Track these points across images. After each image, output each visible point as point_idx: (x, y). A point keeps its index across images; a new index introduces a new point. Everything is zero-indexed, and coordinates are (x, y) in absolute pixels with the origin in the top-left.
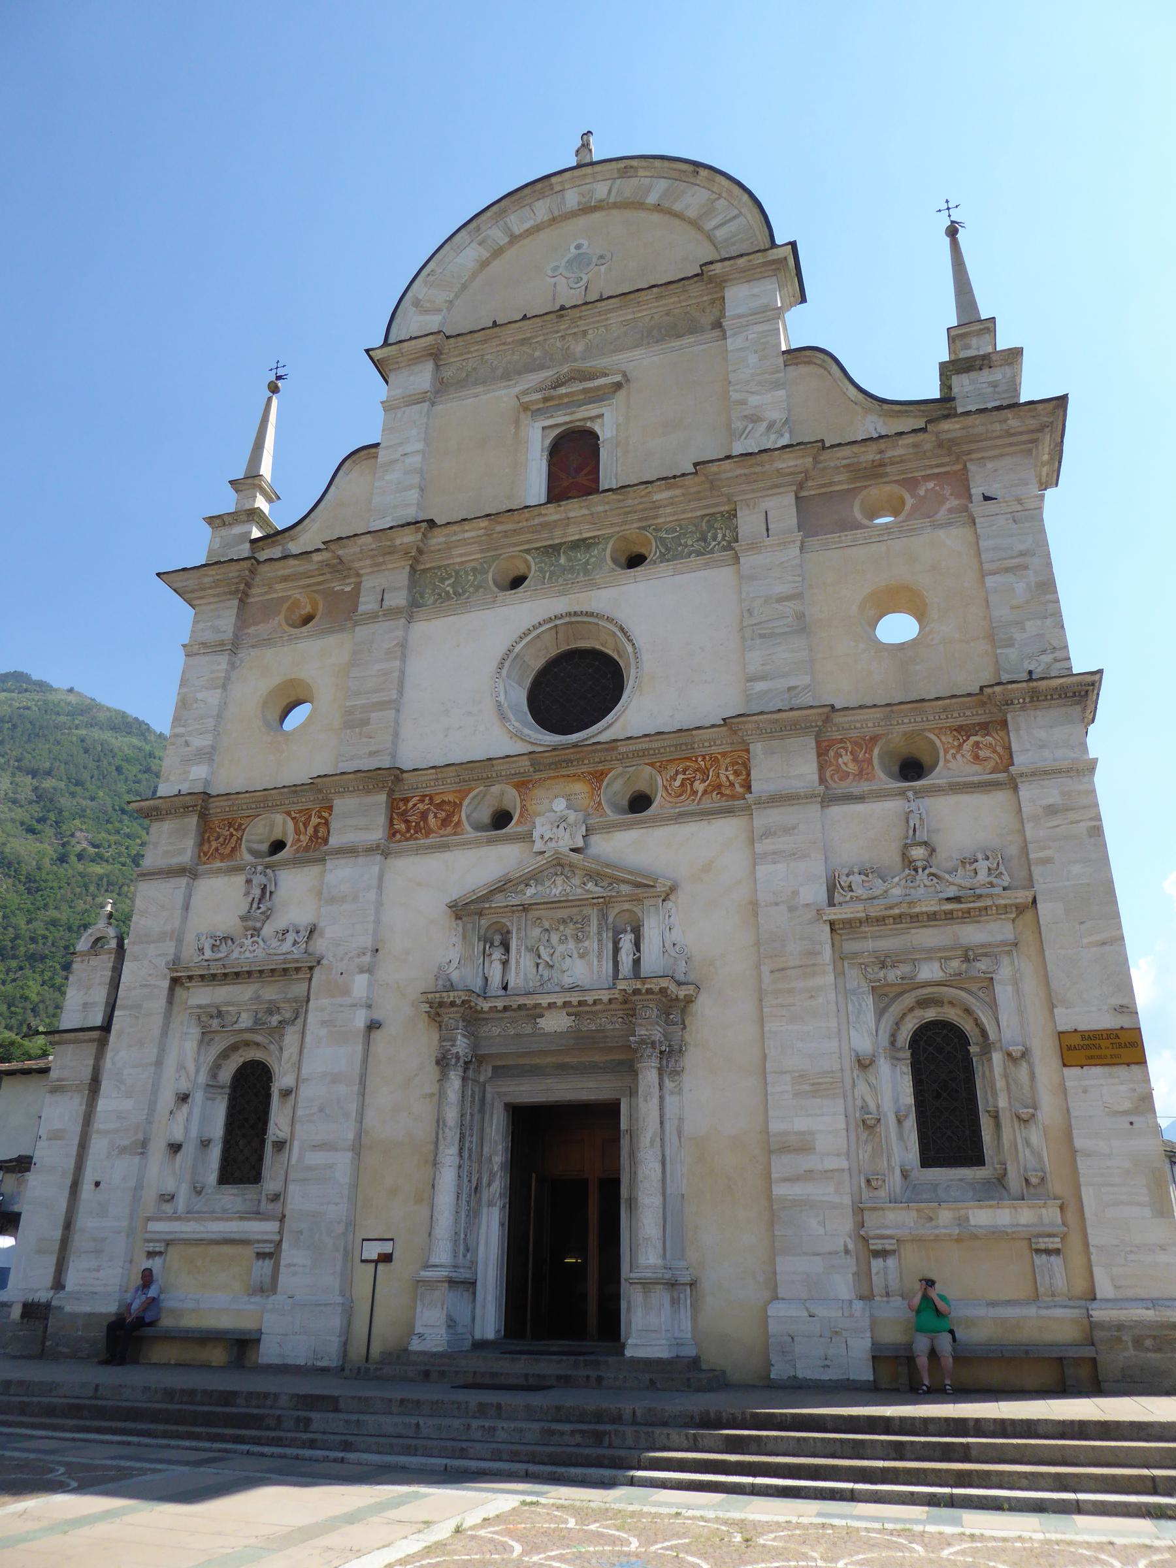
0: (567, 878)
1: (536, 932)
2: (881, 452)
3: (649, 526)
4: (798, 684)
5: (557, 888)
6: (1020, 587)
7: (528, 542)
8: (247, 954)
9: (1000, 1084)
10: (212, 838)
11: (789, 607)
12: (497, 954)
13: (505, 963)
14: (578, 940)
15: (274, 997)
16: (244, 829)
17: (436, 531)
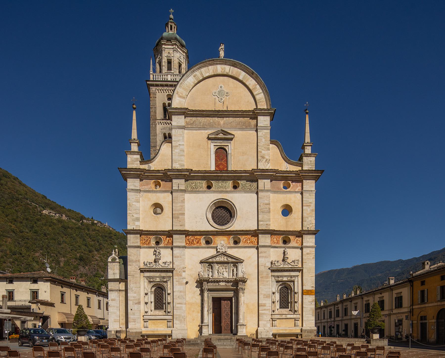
1: (218, 266)
5: (223, 259)
6: (309, 210)
11: (267, 206)
12: (210, 270)
14: (226, 269)
15: (164, 276)
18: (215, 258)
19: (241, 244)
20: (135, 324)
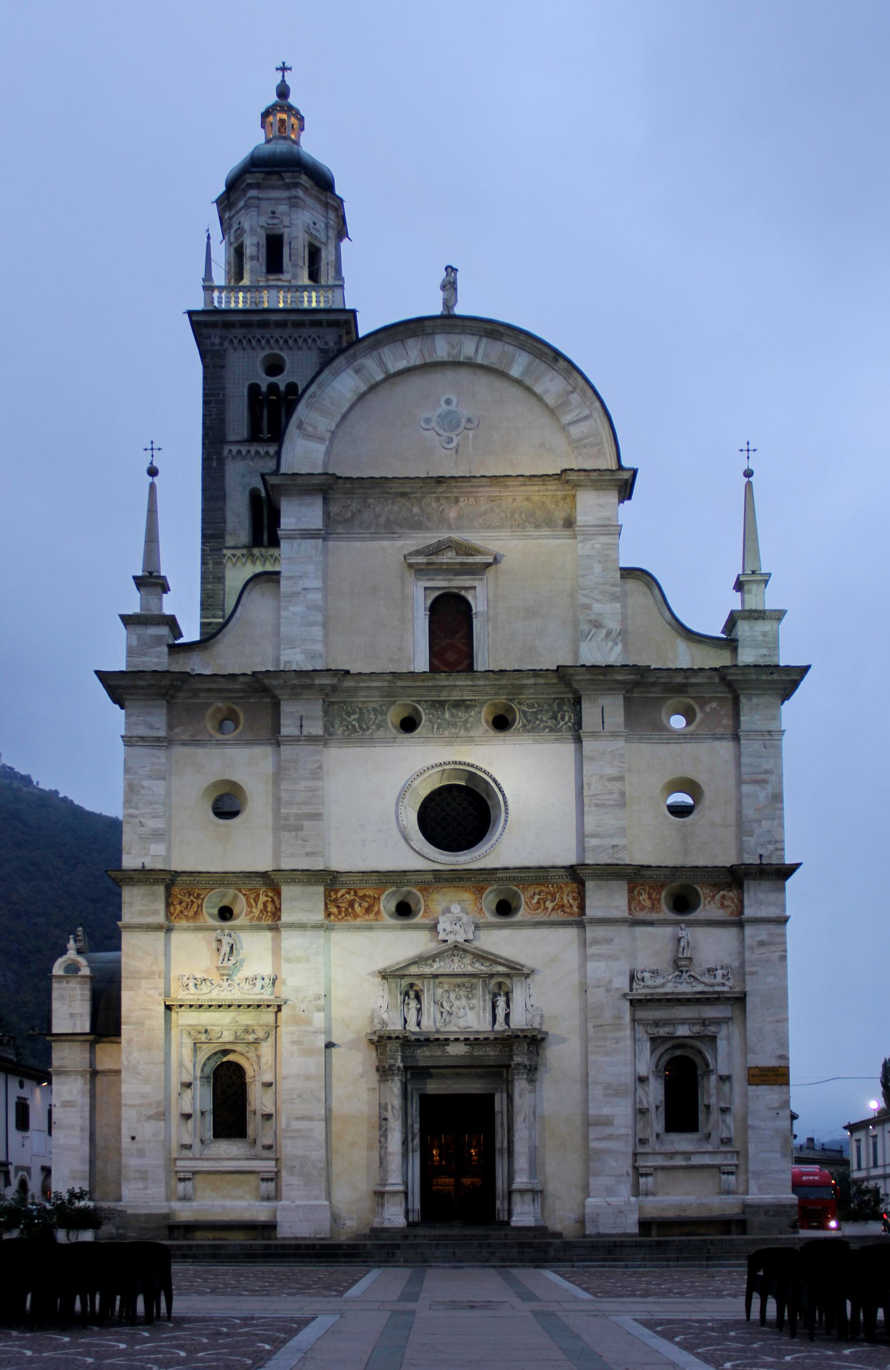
0: (461, 957)
2: (687, 678)
3: (515, 699)
5: (456, 966)
6: (762, 795)
7: (421, 696)
9: (713, 1092)
10: (175, 903)
11: (616, 786)
12: (413, 1004)
13: (419, 1010)
14: (468, 998)
16: (203, 899)
17: (348, 678)
18: (430, 962)
19: (522, 915)
20: (146, 1188)
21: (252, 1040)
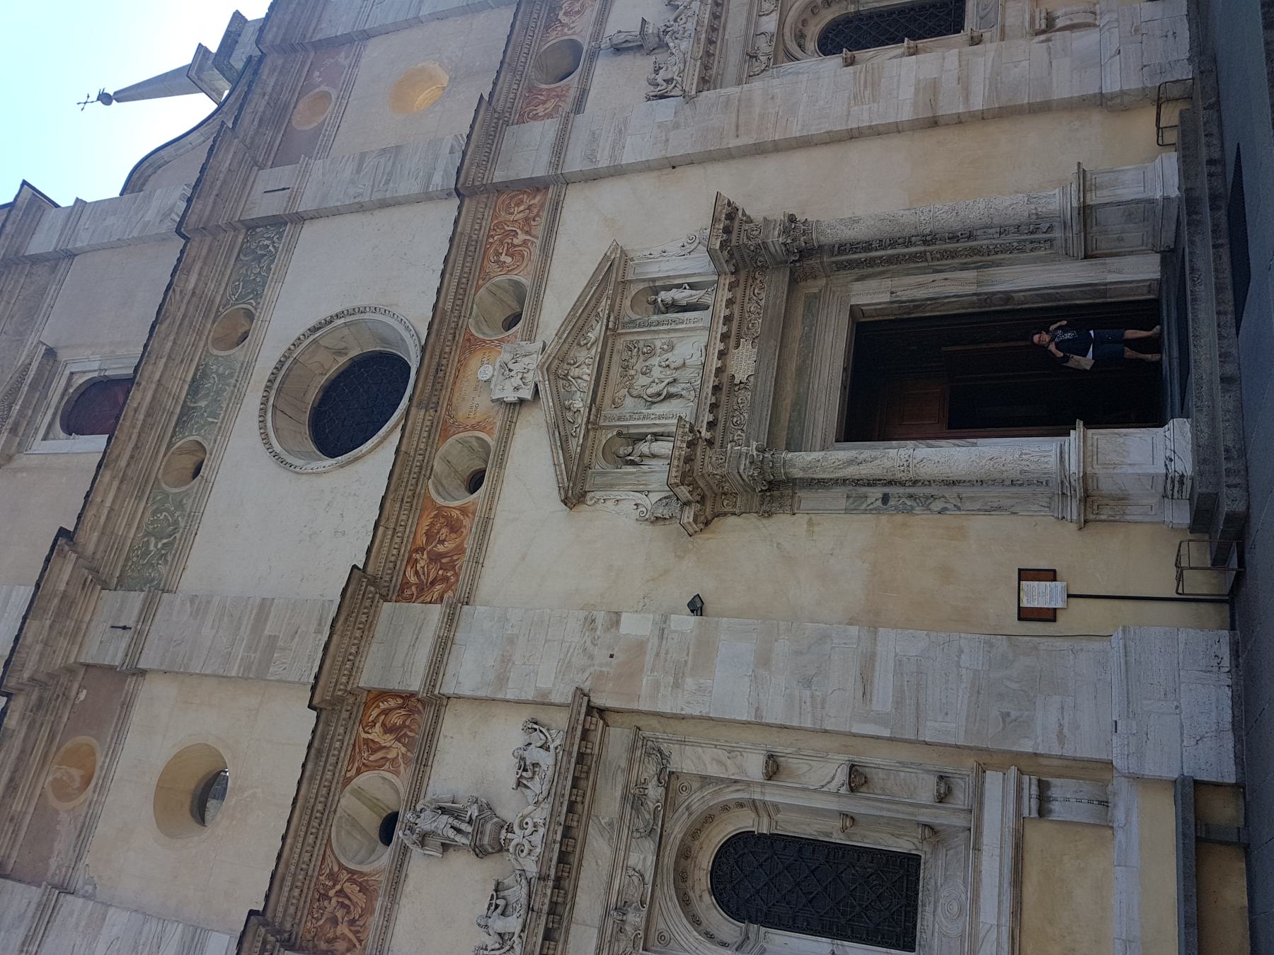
4: (449, 145)
7: (160, 439)
8: (537, 839)
10: (331, 935)
12: (644, 448)
14: (651, 353)
15: (618, 794)
16: (341, 866)
17: (81, 538)
21: (661, 790)
